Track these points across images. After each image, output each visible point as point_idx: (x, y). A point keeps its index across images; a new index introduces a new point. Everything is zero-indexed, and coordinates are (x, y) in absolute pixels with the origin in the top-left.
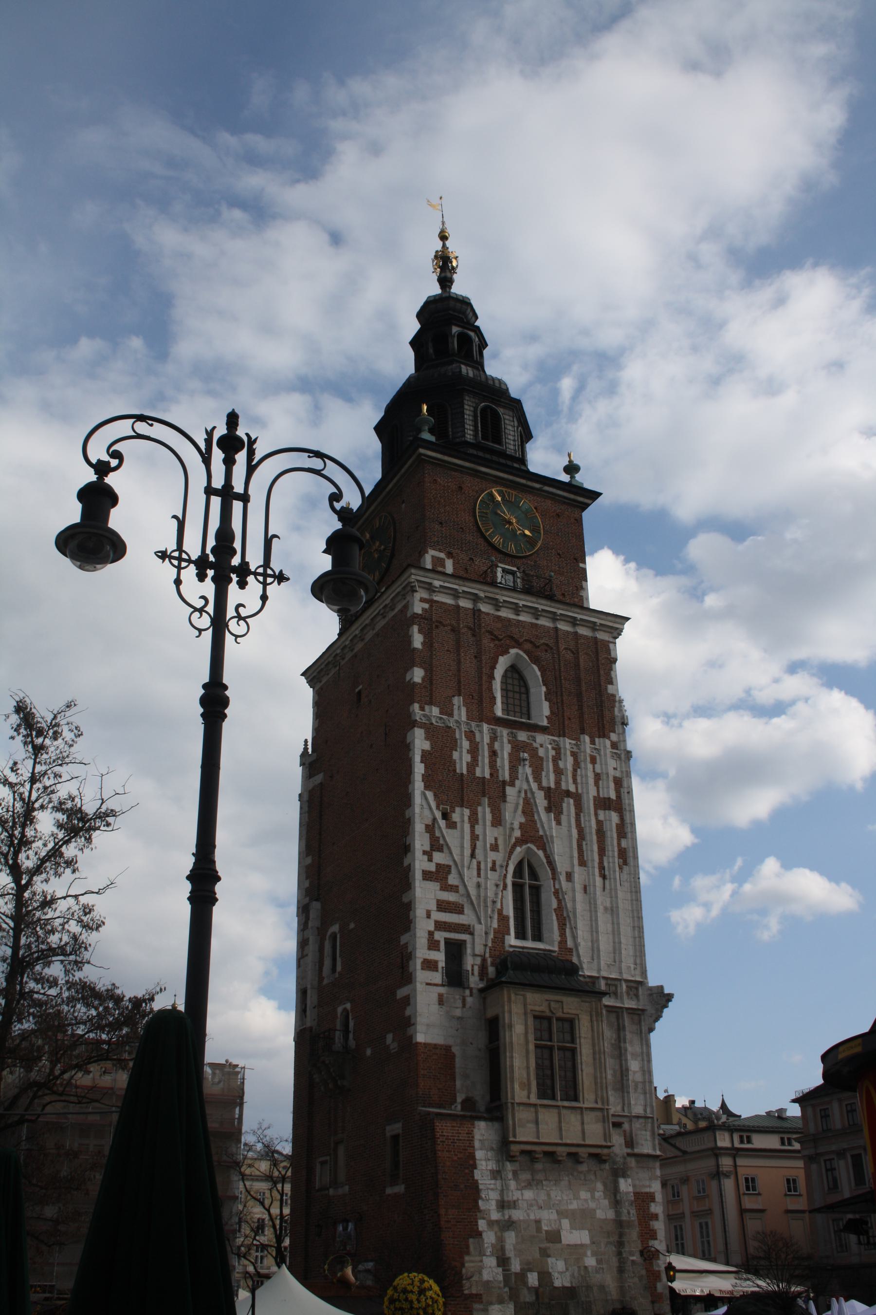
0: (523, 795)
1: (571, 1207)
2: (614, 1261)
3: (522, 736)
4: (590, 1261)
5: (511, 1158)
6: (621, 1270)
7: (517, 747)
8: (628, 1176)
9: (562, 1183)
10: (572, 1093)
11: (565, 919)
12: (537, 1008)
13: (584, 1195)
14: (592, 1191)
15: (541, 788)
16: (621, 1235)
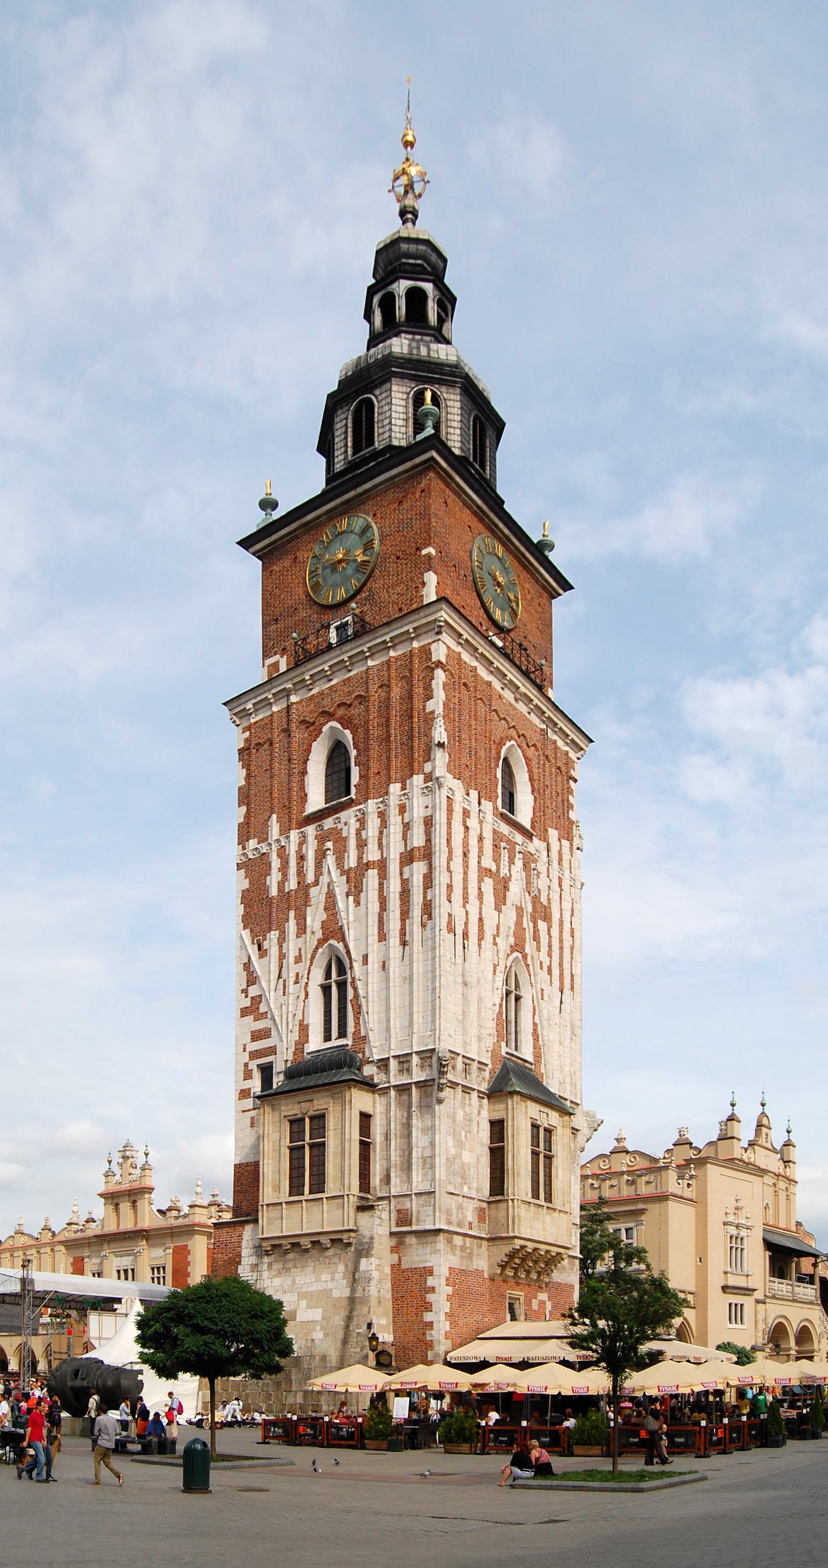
0: (325, 890)
1: (310, 1289)
2: (341, 1334)
3: (328, 823)
4: (318, 1335)
5: (267, 1253)
6: (345, 1342)
7: (322, 839)
8: (372, 1256)
9: (307, 1269)
10: (318, 1185)
11: (360, 1007)
12: (290, 1113)
13: (325, 1277)
14: (333, 1273)
15: (343, 873)
16: (351, 1311)
